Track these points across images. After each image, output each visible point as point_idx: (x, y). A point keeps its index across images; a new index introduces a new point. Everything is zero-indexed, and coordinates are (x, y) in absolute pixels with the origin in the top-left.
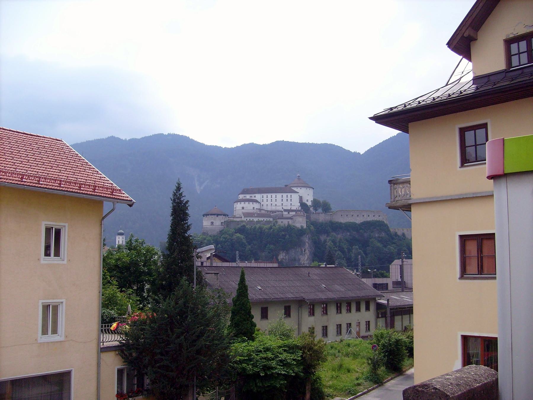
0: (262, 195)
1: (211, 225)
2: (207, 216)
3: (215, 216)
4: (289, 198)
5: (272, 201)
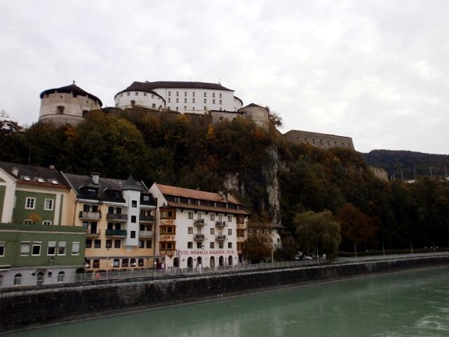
0: (168, 90)
1: (57, 114)
3: (68, 94)
4: (217, 99)
5: (186, 102)
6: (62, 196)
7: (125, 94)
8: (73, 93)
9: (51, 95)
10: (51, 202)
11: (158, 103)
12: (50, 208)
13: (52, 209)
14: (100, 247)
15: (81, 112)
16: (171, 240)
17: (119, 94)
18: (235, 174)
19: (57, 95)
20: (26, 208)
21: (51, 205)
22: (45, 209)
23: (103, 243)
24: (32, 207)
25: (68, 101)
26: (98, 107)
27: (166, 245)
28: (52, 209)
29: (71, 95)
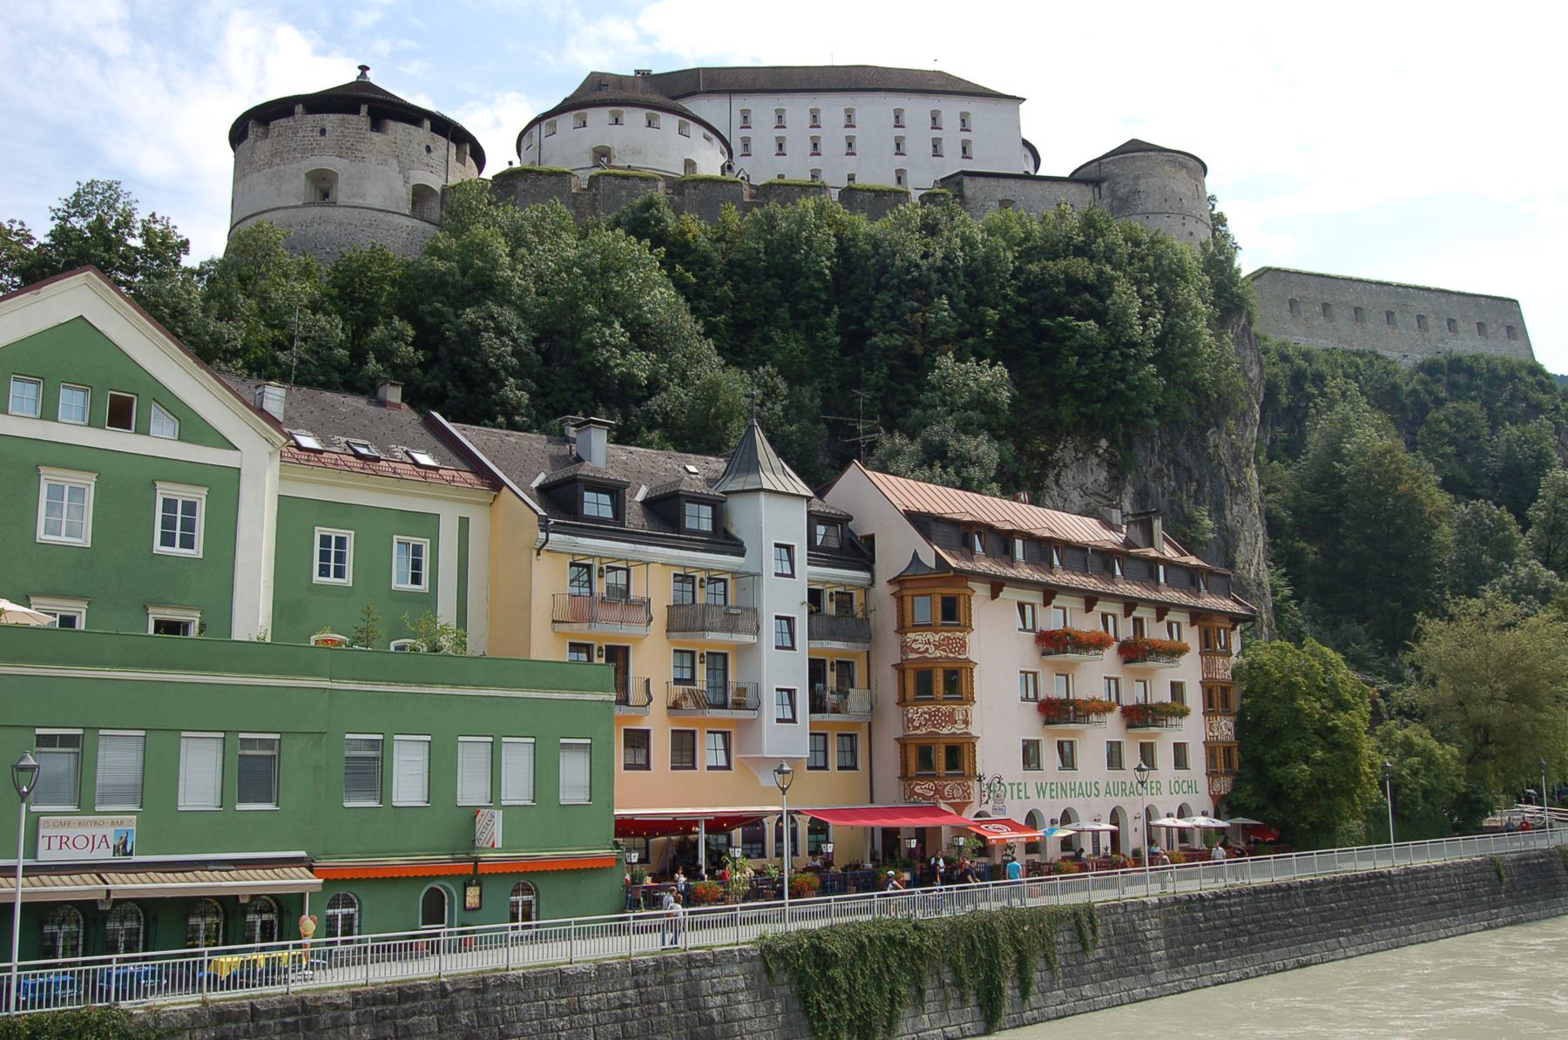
0: (741, 103)
2: (272, 124)
3: (354, 117)
4: (951, 136)
6: (464, 523)
7: (568, 119)
8: (369, 113)
9: (278, 125)
10: (417, 550)
11: (710, 162)
12: (416, 579)
13: (424, 587)
14: (647, 767)
15: (405, 193)
16: (959, 728)
17: (537, 121)
18: (1092, 448)
19: (307, 123)
20: (317, 579)
21: (417, 565)
22: (395, 585)
23: (661, 747)
24: (339, 573)
25: (346, 150)
26: (463, 172)
27: (940, 758)
28: (424, 587)
29: (362, 120)
